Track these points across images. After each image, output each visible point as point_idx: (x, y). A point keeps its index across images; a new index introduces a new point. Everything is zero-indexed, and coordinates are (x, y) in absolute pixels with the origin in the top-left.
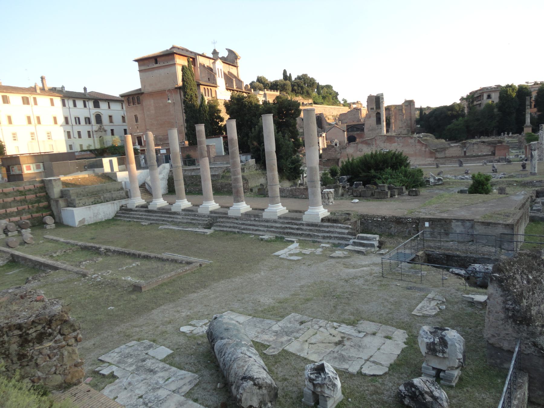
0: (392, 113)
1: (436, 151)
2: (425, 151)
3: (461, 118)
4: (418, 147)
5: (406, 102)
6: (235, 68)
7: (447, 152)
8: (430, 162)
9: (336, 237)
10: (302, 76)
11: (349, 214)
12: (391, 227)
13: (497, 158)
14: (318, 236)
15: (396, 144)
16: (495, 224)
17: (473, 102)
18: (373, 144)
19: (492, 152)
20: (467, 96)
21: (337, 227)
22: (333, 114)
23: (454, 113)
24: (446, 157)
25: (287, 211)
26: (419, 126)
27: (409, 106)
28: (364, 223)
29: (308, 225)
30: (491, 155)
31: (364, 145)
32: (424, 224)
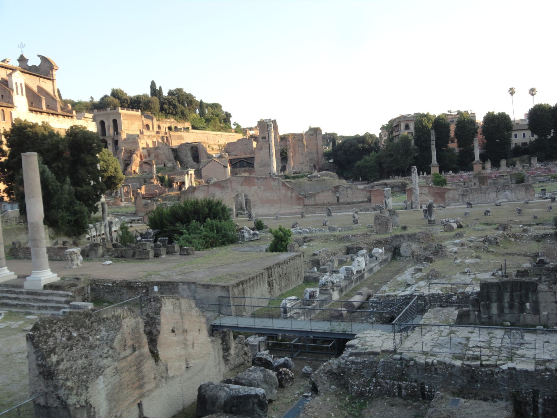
0: (290, 144)
1: (305, 196)
2: (291, 197)
3: (373, 153)
4: (283, 192)
5: (311, 129)
6: (51, 82)
7: (317, 198)
8: (297, 210)
9: (52, 307)
10: (175, 90)
11: (78, 279)
12: (123, 293)
13: (373, 205)
14: (33, 306)
15: (256, 187)
16: (213, 286)
17: (392, 133)
18: (228, 188)
19: (368, 198)
20: (388, 125)
21: (57, 295)
22: (220, 143)
23: (366, 146)
24: (316, 204)
25: (16, 277)
26: (331, 161)
27: (315, 135)
28: (96, 289)
29: (28, 293)
30: (367, 202)
31: (217, 188)
32: (154, 289)
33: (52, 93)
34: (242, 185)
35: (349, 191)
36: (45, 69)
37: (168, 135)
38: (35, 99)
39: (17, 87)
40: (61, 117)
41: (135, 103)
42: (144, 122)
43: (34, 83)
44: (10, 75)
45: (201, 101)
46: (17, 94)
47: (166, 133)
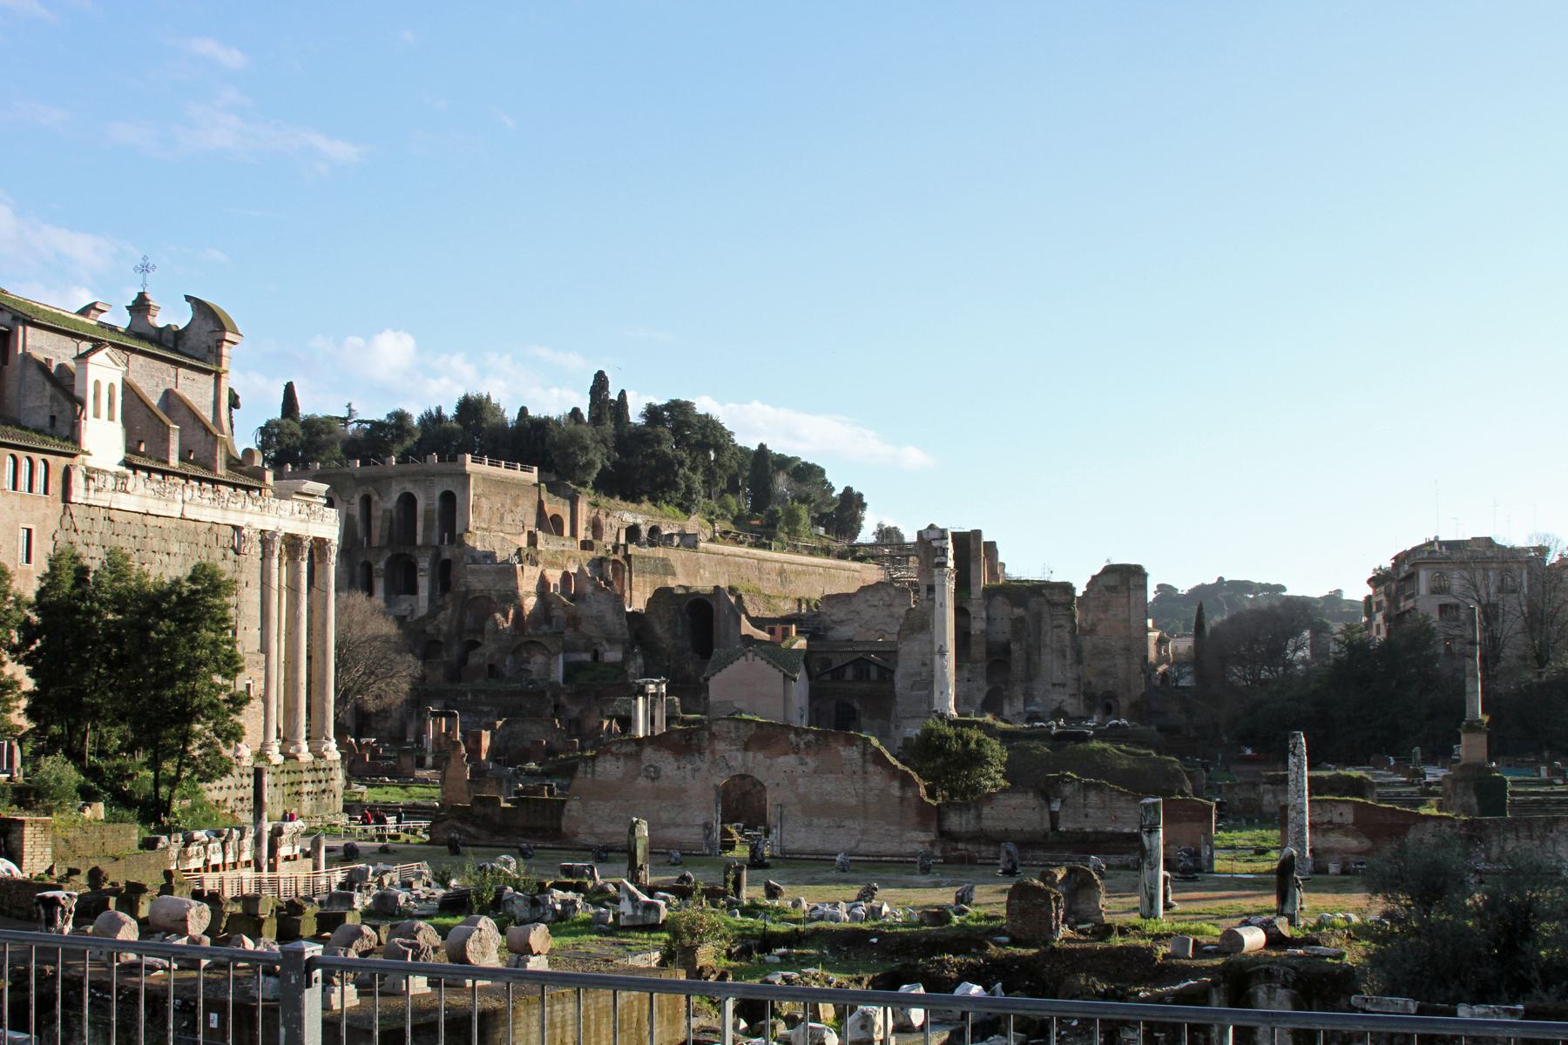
2: (902, 799)
5: (1110, 570)
6: (211, 379)
10: (667, 407)
15: (791, 760)
33: (207, 415)
34: (746, 748)
35: (1093, 797)
36: (200, 341)
37: (619, 557)
38: (154, 434)
39: (96, 397)
40: (226, 491)
41: (529, 442)
42: (547, 507)
43: (154, 379)
44: (82, 358)
45: (762, 447)
46: (97, 415)
47: (616, 548)
